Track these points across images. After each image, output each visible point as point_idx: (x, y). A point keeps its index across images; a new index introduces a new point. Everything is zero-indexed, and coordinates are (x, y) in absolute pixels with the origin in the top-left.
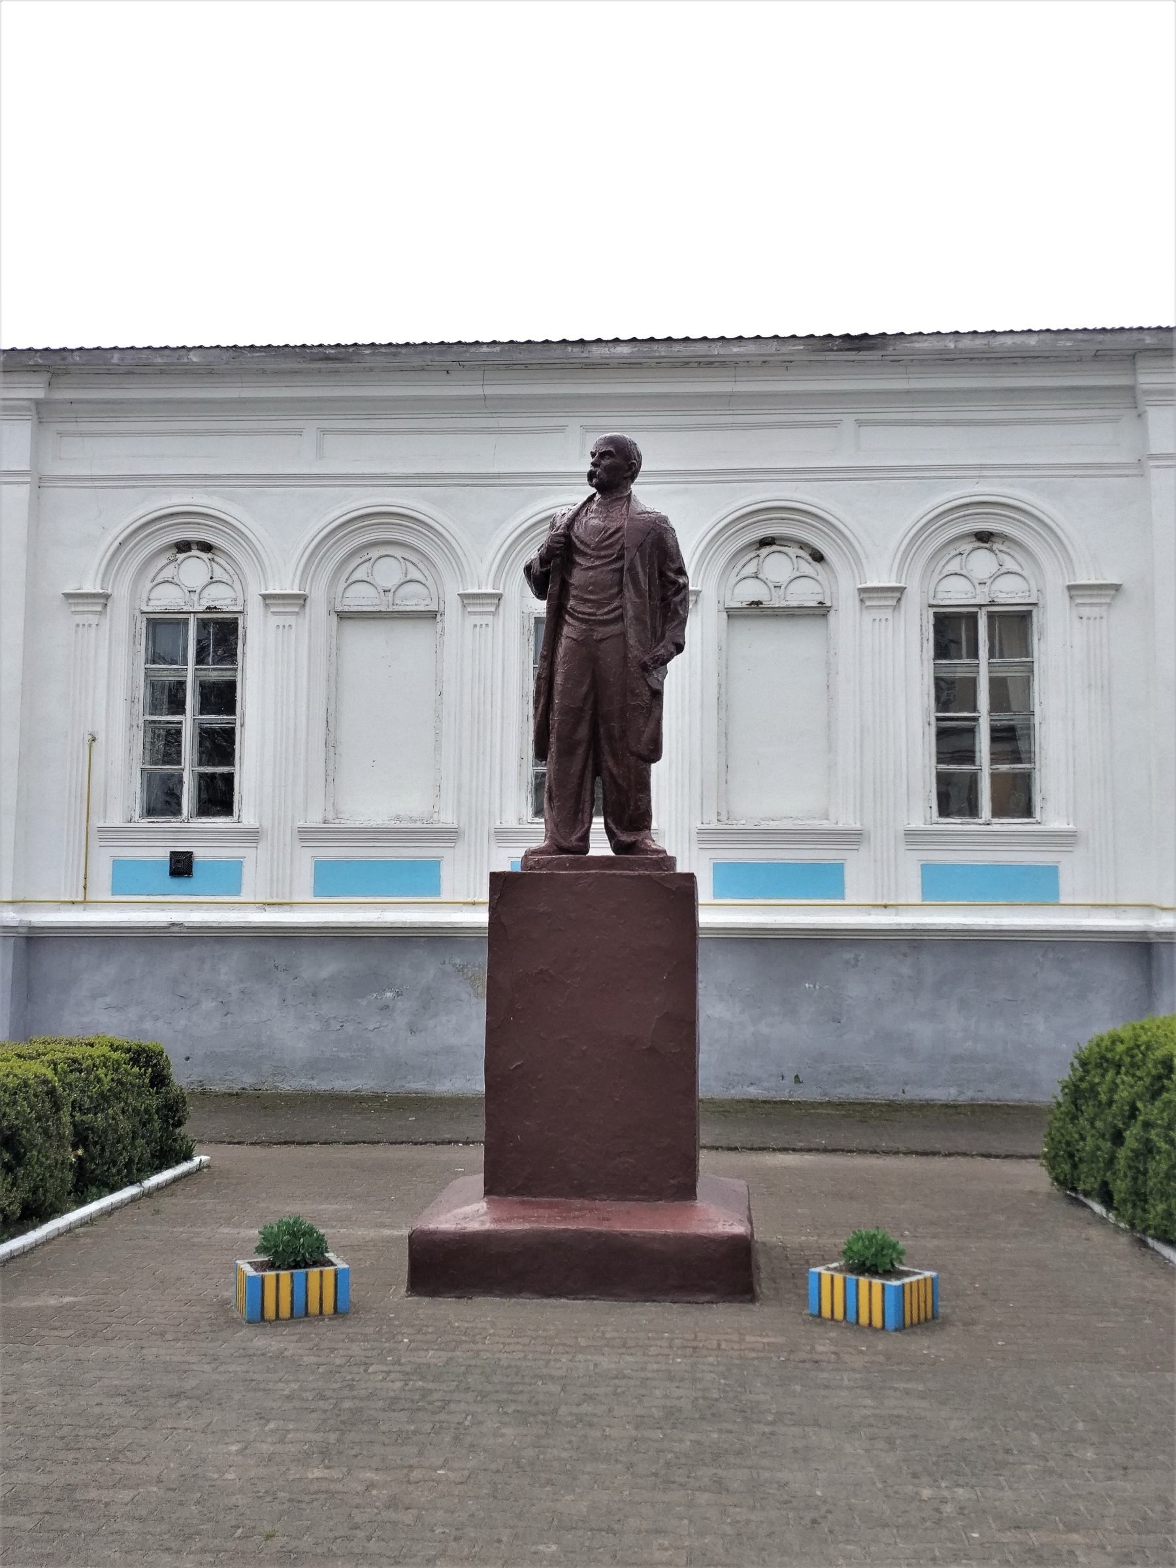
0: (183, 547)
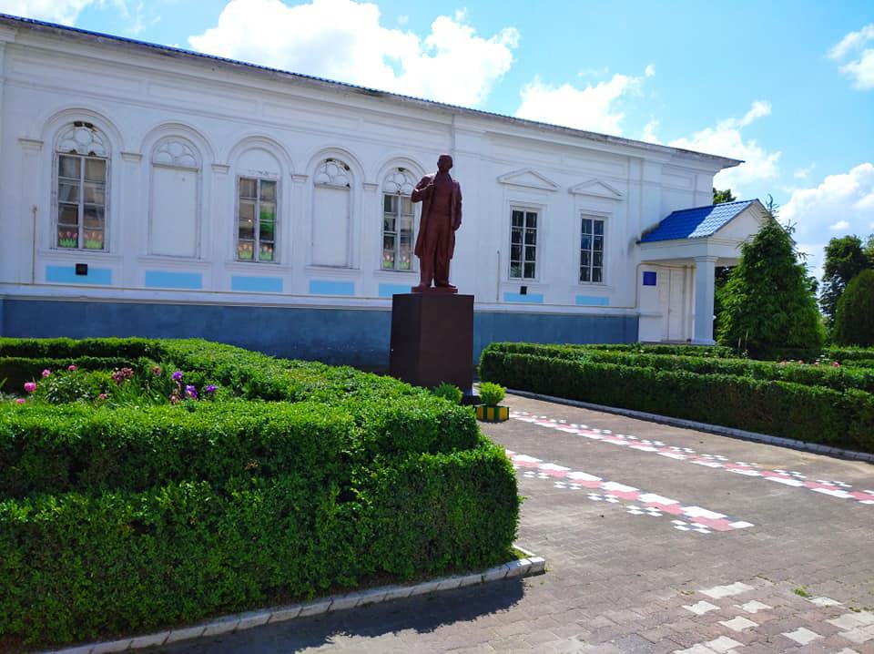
0: (78, 124)
